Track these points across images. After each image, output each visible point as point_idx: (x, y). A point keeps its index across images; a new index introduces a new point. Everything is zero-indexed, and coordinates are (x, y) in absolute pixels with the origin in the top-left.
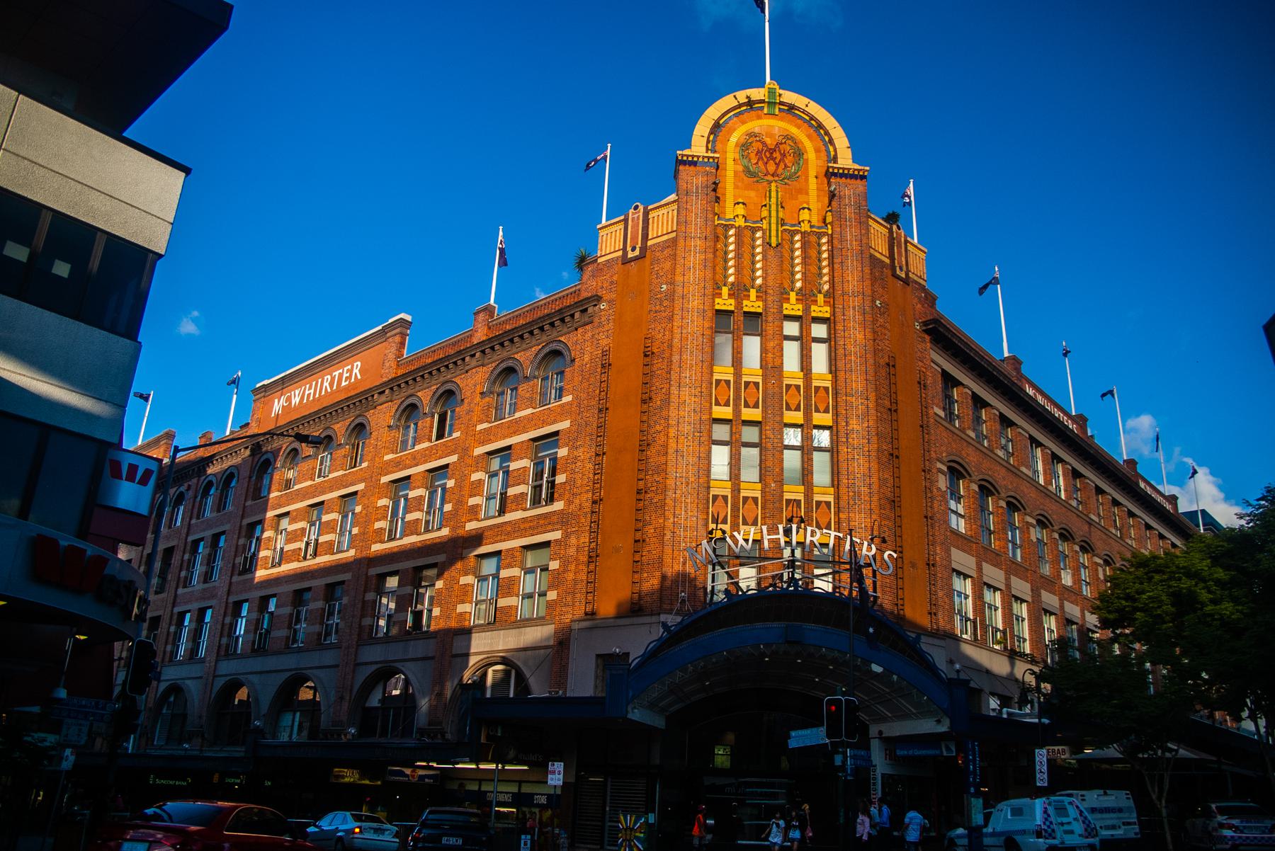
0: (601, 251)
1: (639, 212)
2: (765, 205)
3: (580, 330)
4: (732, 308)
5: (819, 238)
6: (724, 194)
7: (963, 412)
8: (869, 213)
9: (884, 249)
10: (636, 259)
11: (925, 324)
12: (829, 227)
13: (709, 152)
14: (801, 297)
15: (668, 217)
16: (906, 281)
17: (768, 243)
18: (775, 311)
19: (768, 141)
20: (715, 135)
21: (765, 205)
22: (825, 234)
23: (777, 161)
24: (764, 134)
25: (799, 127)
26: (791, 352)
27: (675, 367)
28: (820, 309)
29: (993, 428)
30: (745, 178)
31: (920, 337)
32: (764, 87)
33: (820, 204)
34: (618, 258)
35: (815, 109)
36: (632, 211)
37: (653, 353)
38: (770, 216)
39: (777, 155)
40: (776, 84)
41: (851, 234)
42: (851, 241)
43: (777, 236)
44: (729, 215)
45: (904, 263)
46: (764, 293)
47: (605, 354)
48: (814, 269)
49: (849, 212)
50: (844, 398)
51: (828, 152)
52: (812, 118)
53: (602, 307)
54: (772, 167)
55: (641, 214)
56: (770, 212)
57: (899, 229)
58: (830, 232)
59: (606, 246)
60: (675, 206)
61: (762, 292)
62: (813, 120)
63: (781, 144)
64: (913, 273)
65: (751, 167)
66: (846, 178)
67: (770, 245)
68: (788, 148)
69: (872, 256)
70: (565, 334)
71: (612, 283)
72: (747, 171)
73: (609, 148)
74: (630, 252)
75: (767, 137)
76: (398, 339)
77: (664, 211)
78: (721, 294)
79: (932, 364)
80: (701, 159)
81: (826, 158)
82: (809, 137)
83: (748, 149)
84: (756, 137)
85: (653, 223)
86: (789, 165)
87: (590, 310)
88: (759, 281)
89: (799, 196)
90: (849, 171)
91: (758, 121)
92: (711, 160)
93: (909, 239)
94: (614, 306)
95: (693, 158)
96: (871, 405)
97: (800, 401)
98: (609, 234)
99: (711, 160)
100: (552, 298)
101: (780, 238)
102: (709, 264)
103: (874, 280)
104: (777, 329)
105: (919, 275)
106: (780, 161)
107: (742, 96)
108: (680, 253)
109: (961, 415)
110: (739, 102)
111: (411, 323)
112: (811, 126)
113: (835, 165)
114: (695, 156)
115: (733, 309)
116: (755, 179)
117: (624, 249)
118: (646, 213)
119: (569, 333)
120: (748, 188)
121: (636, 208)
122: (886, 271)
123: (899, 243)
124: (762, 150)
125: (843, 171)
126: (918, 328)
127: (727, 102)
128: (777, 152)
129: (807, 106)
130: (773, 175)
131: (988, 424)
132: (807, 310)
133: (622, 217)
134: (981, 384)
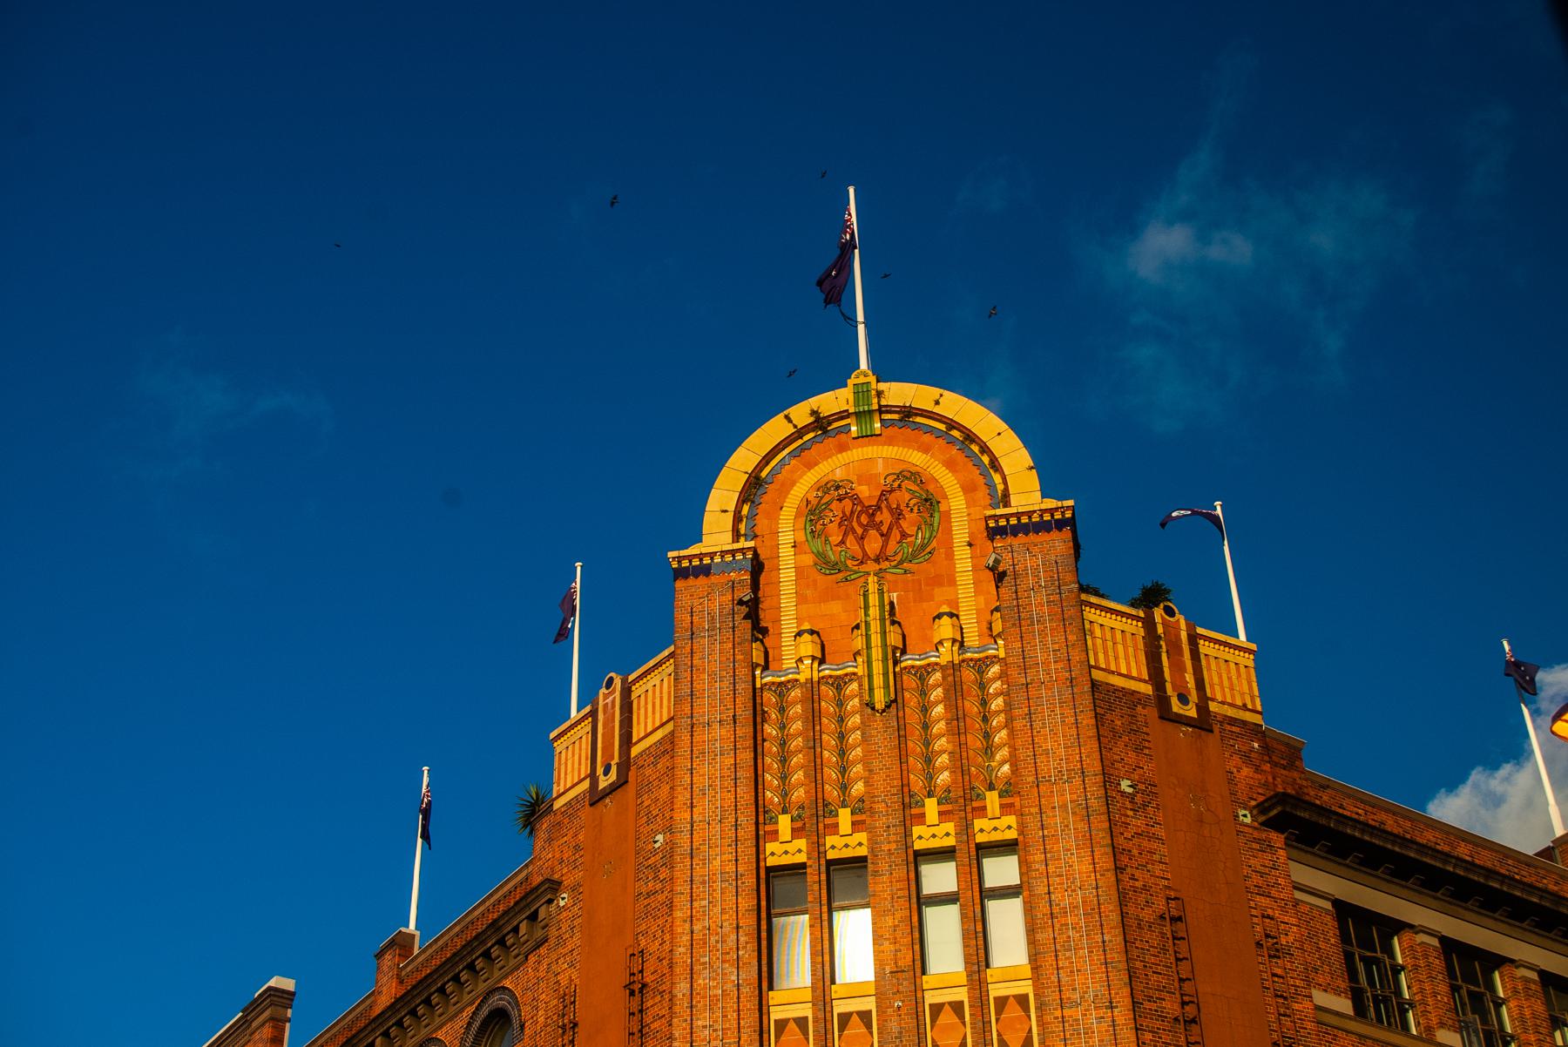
0: (559, 785)
1: (614, 691)
2: (857, 627)
3: (532, 959)
4: (801, 858)
5: (981, 672)
7: (1422, 991)
8: (1084, 597)
9: (1133, 664)
10: (613, 788)
11: (1262, 808)
12: (1000, 642)
13: (742, 539)
14: (949, 807)
15: (661, 693)
16: (1204, 722)
17: (867, 705)
18: (893, 846)
19: (864, 491)
20: (753, 502)
21: (857, 627)
22: (994, 659)
23: (884, 529)
24: (854, 479)
25: (925, 449)
26: (943, 926)
27: (681, 1006)
28: (995, 823)
29: (1527, 1012)
30: (820, 577)
31: (1255, 840)
32: (846, 386)
33: (982, 599)
34: (584, 792)
35: (956, 406)
36: (603, 690)
37: (644, 985)
38: (869, 647)
39: (884, 517)
40: (870, 373)
41: (1046, 648)
42: (1046, 663)
43: (886, 686)
44: (789, 663)
45: (1191, 684)
46: (868, 813)
47: (568, 1000)
48: (975, 741)
49: (1038, 602)
50: (1058, 1013)
51: (991, 486)
52: (952, 425)
53: (562, 903)
54: (873, 544)
55: (617, 694)
56: (868, 637)
57: (1169, 612)
59: (566, 774)
60: (669, 667)
61: (861, 810)
62: (954, 428)
63: (891, 492)
64: (1223, 703)
65: (830, 553)
67: (873, 709)
68: (907, 496)
69: (1095, 685)
70: (512, 972)
71: (577, 848)
73: (579, 569)
74: (602, 777)
75: (859, 485)
76: (267, 1031)
77: (654, 679)
78: (777, 832)
79: (1298, 895)
80: (717, 560)
82: (950, 465)
84: (838, 488)
85: (639, 709)
87: (542, 914)
88: (858, 788)
89: (937, 591)
90: (1030, 517)
91: (839, 456)
92: (739, 557)
93: (1200, 630)
94: (581, 897)
95: (701, 560)
96: (1120, 1020)
97: (965, 1037)
98: (570, 748)
99: (739, 557)
100: (492, 900)
101: (892, 689)
102: (745, 774)
103: (1104, 735)
104: (899, 885)
106: (890, 528)
107: (800, 414)
108: (683, 762)
109: (1417, 998)
110: (795, 426)
111: (293, 994)
112: (952, 442)
113: (1001, 511)
114: (706, 555)
115: (804, 860)
116: (841, 576)
117: (593, 776)
118: (627, 691)
119: (517, 968)
120: (827, 596)
121: (610, 682)
122: (1145, 712)
123: (1175, 648)
124: (852, 512)
125: (1019, 519)
126: (1248, 820)
127: (774, 430)
128: (885, 510)
129: (937, 403)
130: (877, 560)
131: (1512, 1004)
132: (966, 829)
133: (588, 709)
134: (1468, 915)
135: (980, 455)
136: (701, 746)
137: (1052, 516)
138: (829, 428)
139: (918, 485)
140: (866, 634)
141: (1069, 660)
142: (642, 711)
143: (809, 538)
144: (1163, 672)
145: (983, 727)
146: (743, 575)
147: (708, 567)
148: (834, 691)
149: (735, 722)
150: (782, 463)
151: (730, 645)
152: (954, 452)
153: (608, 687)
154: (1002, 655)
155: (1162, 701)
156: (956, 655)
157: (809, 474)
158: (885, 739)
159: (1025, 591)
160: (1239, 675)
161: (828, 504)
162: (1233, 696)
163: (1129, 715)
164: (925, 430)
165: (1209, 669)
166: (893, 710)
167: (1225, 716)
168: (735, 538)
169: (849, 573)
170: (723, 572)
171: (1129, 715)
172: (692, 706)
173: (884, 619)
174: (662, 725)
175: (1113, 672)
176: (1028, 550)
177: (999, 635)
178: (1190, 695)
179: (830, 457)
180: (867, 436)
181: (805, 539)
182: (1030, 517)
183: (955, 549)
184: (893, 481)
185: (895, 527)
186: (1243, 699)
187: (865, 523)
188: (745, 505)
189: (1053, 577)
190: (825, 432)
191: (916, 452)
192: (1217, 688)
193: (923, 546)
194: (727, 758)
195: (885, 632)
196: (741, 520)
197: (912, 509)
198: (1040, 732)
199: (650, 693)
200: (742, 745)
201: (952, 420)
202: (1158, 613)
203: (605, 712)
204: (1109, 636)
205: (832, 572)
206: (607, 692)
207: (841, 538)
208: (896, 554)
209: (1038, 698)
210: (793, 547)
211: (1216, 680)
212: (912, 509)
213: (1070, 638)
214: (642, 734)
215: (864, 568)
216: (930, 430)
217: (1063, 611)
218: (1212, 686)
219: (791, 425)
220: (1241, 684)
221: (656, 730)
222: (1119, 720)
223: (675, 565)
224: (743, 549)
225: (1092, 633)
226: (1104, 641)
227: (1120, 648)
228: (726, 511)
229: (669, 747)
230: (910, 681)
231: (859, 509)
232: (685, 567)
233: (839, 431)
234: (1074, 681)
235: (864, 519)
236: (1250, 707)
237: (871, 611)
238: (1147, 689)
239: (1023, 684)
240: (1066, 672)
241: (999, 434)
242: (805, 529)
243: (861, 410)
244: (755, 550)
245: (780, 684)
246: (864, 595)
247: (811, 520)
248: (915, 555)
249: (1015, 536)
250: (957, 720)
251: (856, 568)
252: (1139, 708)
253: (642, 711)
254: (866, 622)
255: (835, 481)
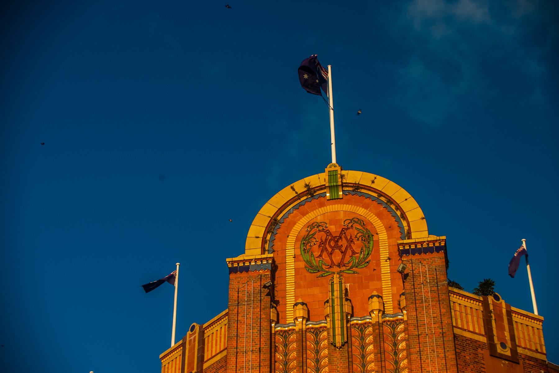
1: (195, 333)
2: (327, 302)
5: (394, 328)
6: (284, 297)
8: (450, 288)
9: (476, 326)
12: (405, 312)
13: (267, 252)
15: (221, 334)
16: (514, 359)
17: (332, 344)
19: (333, 228)
21: (327, 302)
23: (343, 249)
24: (327, 221)
25: (366, 207)
30: (308, 275)
32: (324, 172)
33: (395, 288)
36: (189, 333)
38: (333, 313)
39: (343, 243)
40: (337, 165)
43: (342, 334)
44: (290, 320)
49: (425, 292)
51: (401, 227)
52: (381, 194)
54: (337, 257)
55: (197, 335)
57: (497, 298)
58: (405, 319)
60: (225, 321)
63: (347, 229)
64: (525, 348)
65: (314, 261)
66: (420, 254)
67: (335, 346)
68: (356, 232)
69: (455, 336)
72: (310, 267)
73: (178, 266)
75: (331, 225)
77: (217, 327)
80: (253, 263)
81: (399, 235)
82: (379, 215)
83: (309, 242)
84: (319, 226)
85: (208, 343)
86: (358, 250)
89: (371, 283)
90: (422, 245)
91: (320, 209)
92: (265, 262)
93: (513, 308)
95: (244, 263)
98: (170, 363)
99: (265, 262)
101: (345, 336)
105: (534, 349)
106: (346, 249)
107: (300, 186)
110: (296, 193)
112: (381, 203)
116: (319, 274)
118: (202, 333)
120: (311, 285)
121: (193, 328)
123: (499, 317)
124: (326, 240)
125: (416, 246)
128: (344, 239)
129: (373, 182)
130: (339, 266)
133: (181, 342)
135: (395, 211)
136: (241, 364)
137: (434, 244)
138: (315, 194)
139: (362, 226)
140: (332, 306)
141: (442, 323)
142: (210, 344)
143: (303, 253)
144: (492, 331)
145: (394, 358)
146: (266, 272)
147: (248, 267)
148: (314, 336)
149: (260, 352)
150: (289, 212)
151: (259, 310)
152: (382, 208)
153: (192, 331)
154: (405, 319)
155: (492, 346)
156: (380, 318)
157: (303, 219)
158: (341, 363)
159: (418, 285)
160: (534, 333)
161: (313, 235)
162: (530, 345)
163: (473, 353)
164: (366, 196)
165: (518, 329)
166: (346, 347)
167: (526, 355)
168: (263, 252)
169: (323, 272)
170: (256, 270)
171: (473, 353)
172: (237, 342)
173: (342, 298)
174: (221, 352)
175: (465, 330)
176: (420, 262)
177: (404, 308)
178: (507, 344)
179: (315, 209)
180: (335, 199)
181: (300, 253)
182: (422, 245)
183: (381, 261)
184: (349, 224)
185: (349, 248)
186: (536, 347)
187: (333, 246)
188: (268, 234)
189: (434, 277)
190: (312, 196)
191: (361, 208)
192: (522, 340)
193: (365, 259)
194: (255, 371)
195: (342, 305)
196: (266, 242)
197: (358, 239)
198: (425, 361)
199: (215, 334)
200: (264, 364)
201: (381, 191)
202: (490, 299)
203: (190, 344)
204: (463, 310)
205: (315, 271)
206: (191, 333)
207: (320, 253)
208: (349, 262)
209: (424, 343)
210: (294, 257)
211: (521, 336)
212: (358, 239)
213: (442, 310)
214: (210, 357)
215: (332, 270)
216: (369, 197)
217: (439, 296)
218: (519, 339)
219: (294, 192)
220: (535, 338)
221: (217, 354)
222: (468, 356)
223: (230, 266)
224: (267, 258)
225: (454, 306)
226: (461, 313)
227: (470, 317)
228: (258, 237)
229: (224, 364)
230: (355, 332)
231: (330, 238)
232: (236, 267)
233: (320, 196)
234: (444, 334)
235: (332, 244)
236: (539, 350)
237: (335, 293)
238: (484, 340)
239: (416, 335)
240: (440, 329)
241: (406, 200)
242: (301, 248)
243: (332, 185)
244: (273, 259)
245: (285, 331)
246: (332, 284)
247: (304, 243)
248: (359, 264)
249: (414, 255)
250: (380, 353)
251: (327, 270)
252: (479, 350)
253: (210, 344)
254: (332, 299)
255: (318, 223)
